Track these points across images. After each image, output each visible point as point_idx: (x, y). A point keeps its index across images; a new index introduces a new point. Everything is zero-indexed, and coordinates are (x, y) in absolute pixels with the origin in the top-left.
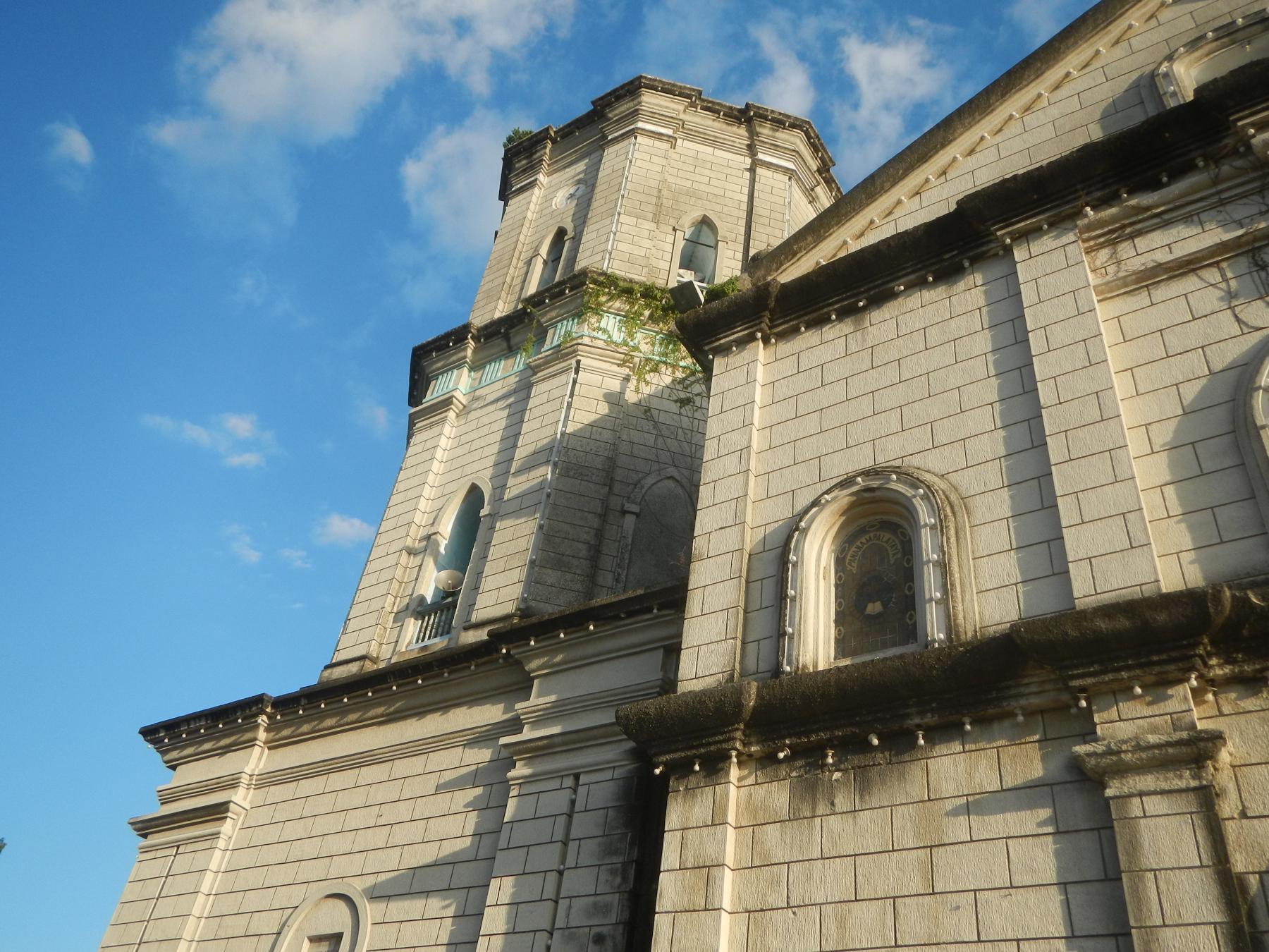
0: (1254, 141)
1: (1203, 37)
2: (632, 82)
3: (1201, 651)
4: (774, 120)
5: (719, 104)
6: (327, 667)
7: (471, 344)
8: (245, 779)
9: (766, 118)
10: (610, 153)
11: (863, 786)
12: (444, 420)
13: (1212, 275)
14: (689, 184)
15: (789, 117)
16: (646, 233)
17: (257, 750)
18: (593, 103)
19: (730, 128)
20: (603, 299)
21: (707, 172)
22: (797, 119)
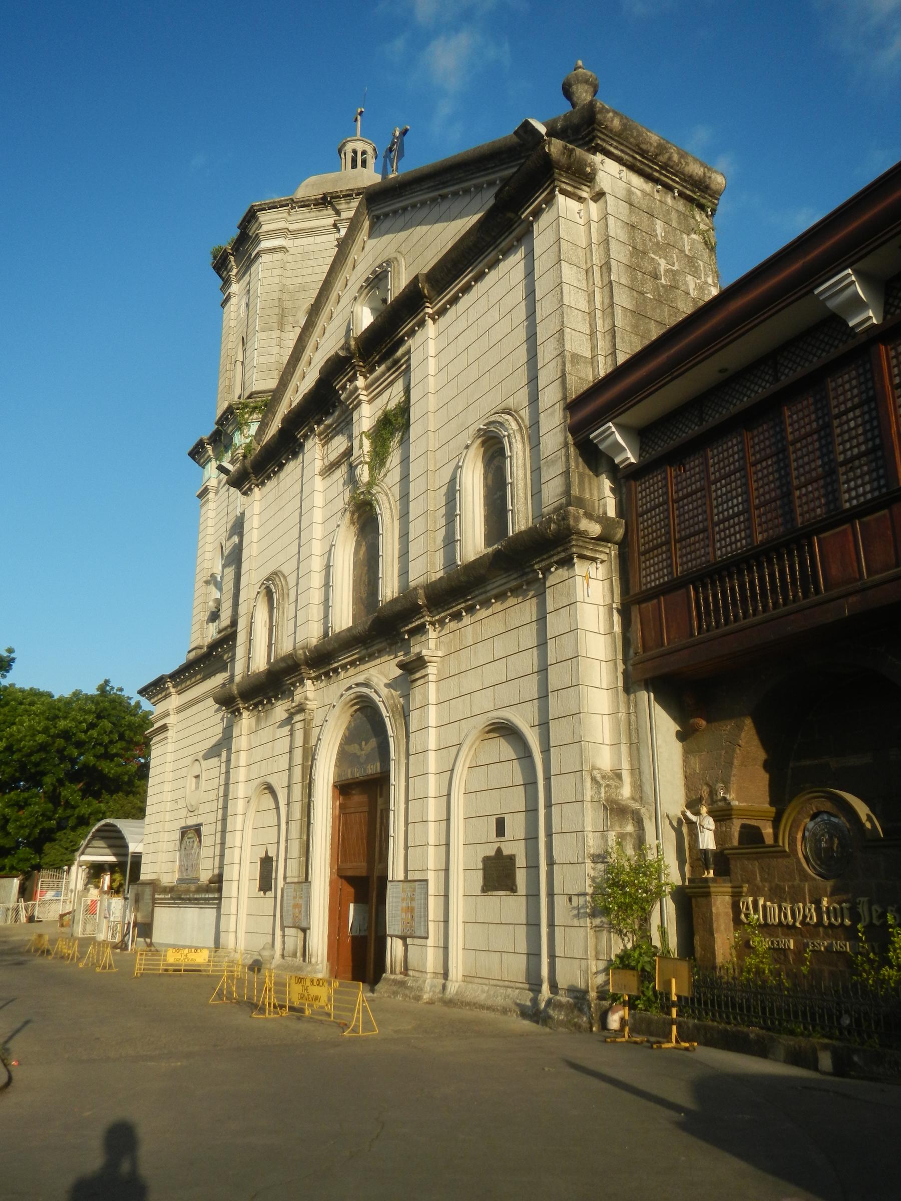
0: (342, 397)
1: (362, 286)
2: (250, 211)
3: (303, 671)
4: (344, 196)
5: (308, 200)
6: (189, 652)
7: (209, 447)
8: (171, 712)
9: (339, 197)
10: (253, 268)
11: (266, 717)
12: (207, 501)
13: (343, 466)
14: (299, 280)
15: (352, 190)
16: (274, 342)
17: (173, 697)
18: (239, 228)
19: (321, 213)
20: (246, 416)
21: (311, 263)
22: (359, 189)
